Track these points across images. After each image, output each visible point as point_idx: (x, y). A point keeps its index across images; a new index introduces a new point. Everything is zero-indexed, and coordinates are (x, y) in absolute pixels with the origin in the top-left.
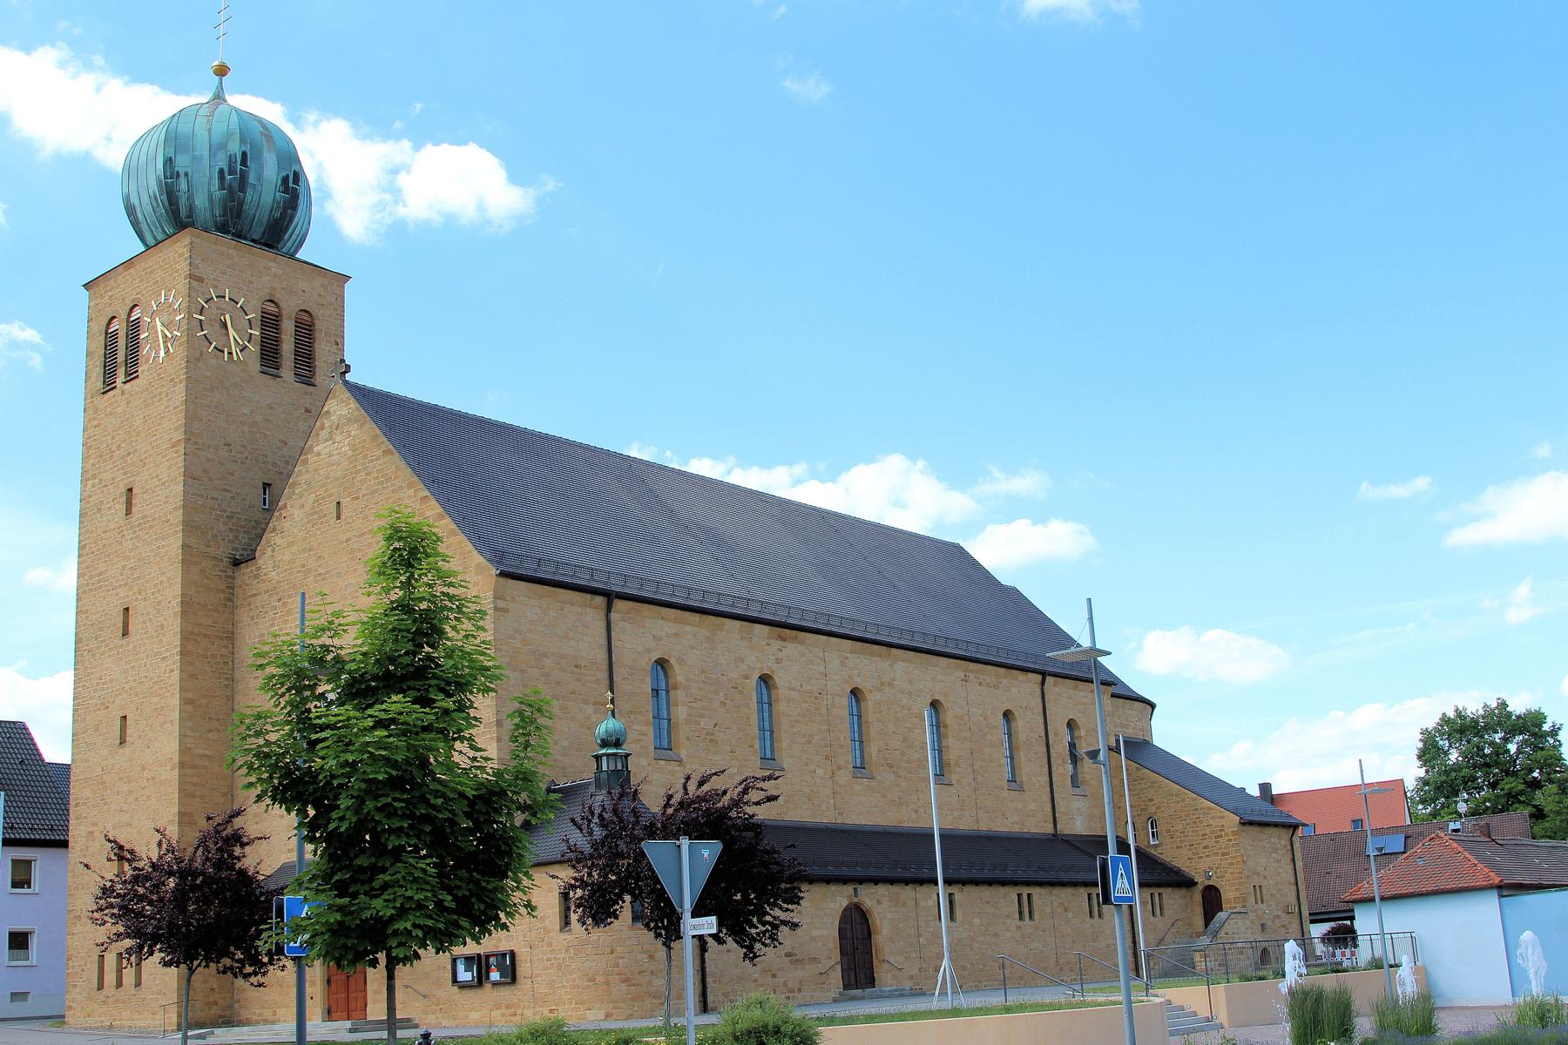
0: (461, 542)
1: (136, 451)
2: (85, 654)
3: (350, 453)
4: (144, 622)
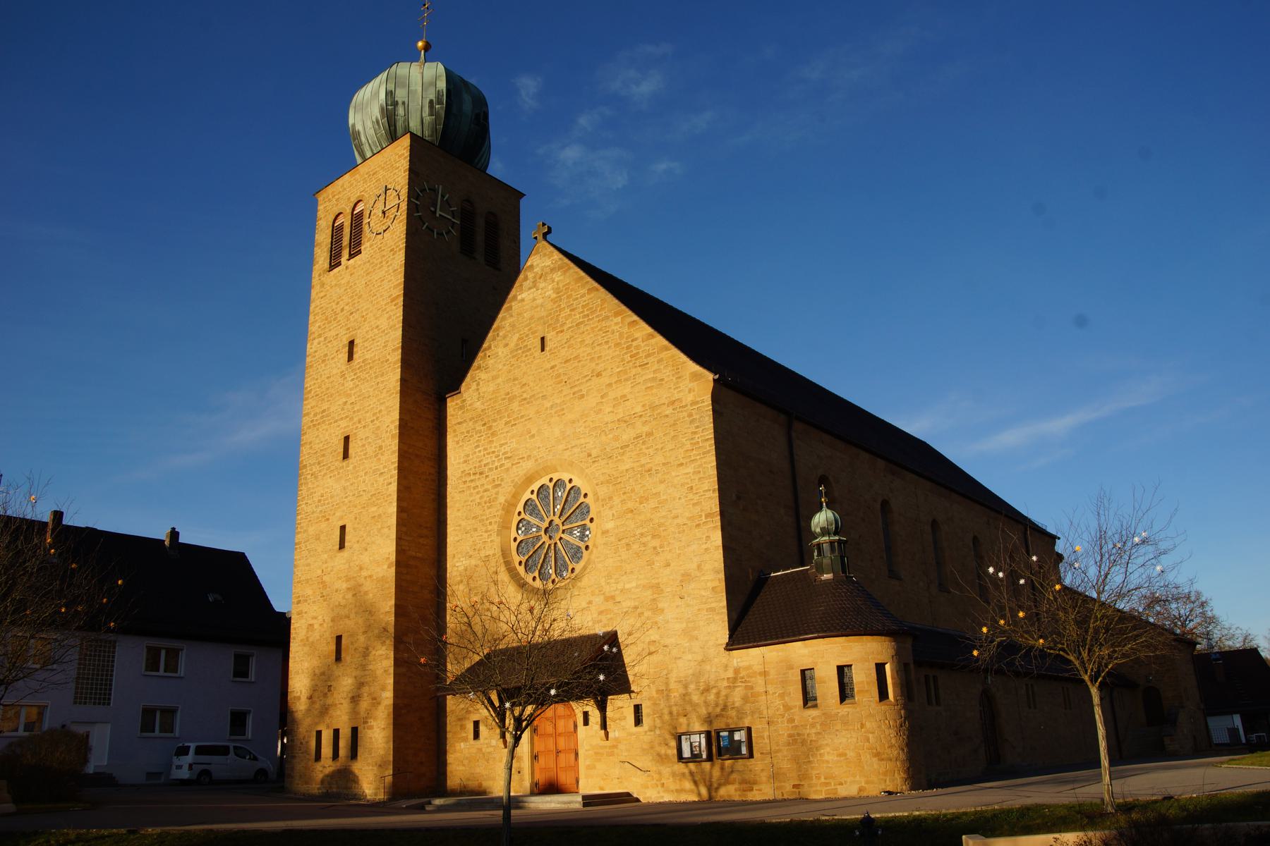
0: (673, 356)
1: (358, 310)
2: (309, 477)
3: (555, 296)
4: (364, 445)
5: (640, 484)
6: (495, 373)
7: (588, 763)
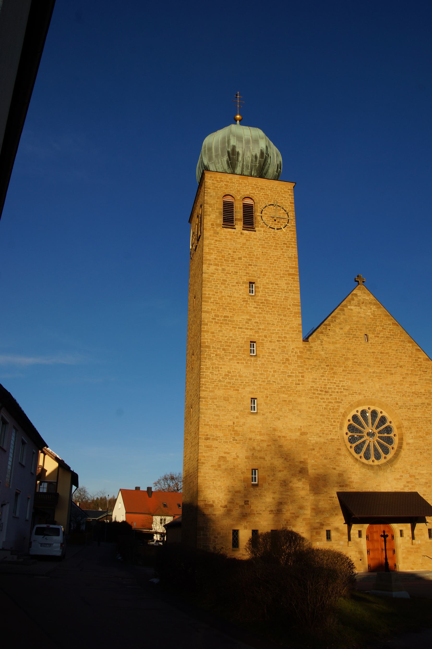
1: (257, 266)
3: (372, 317)
5: (426, 426)
6: (334, 340)
7: (404, 556)
